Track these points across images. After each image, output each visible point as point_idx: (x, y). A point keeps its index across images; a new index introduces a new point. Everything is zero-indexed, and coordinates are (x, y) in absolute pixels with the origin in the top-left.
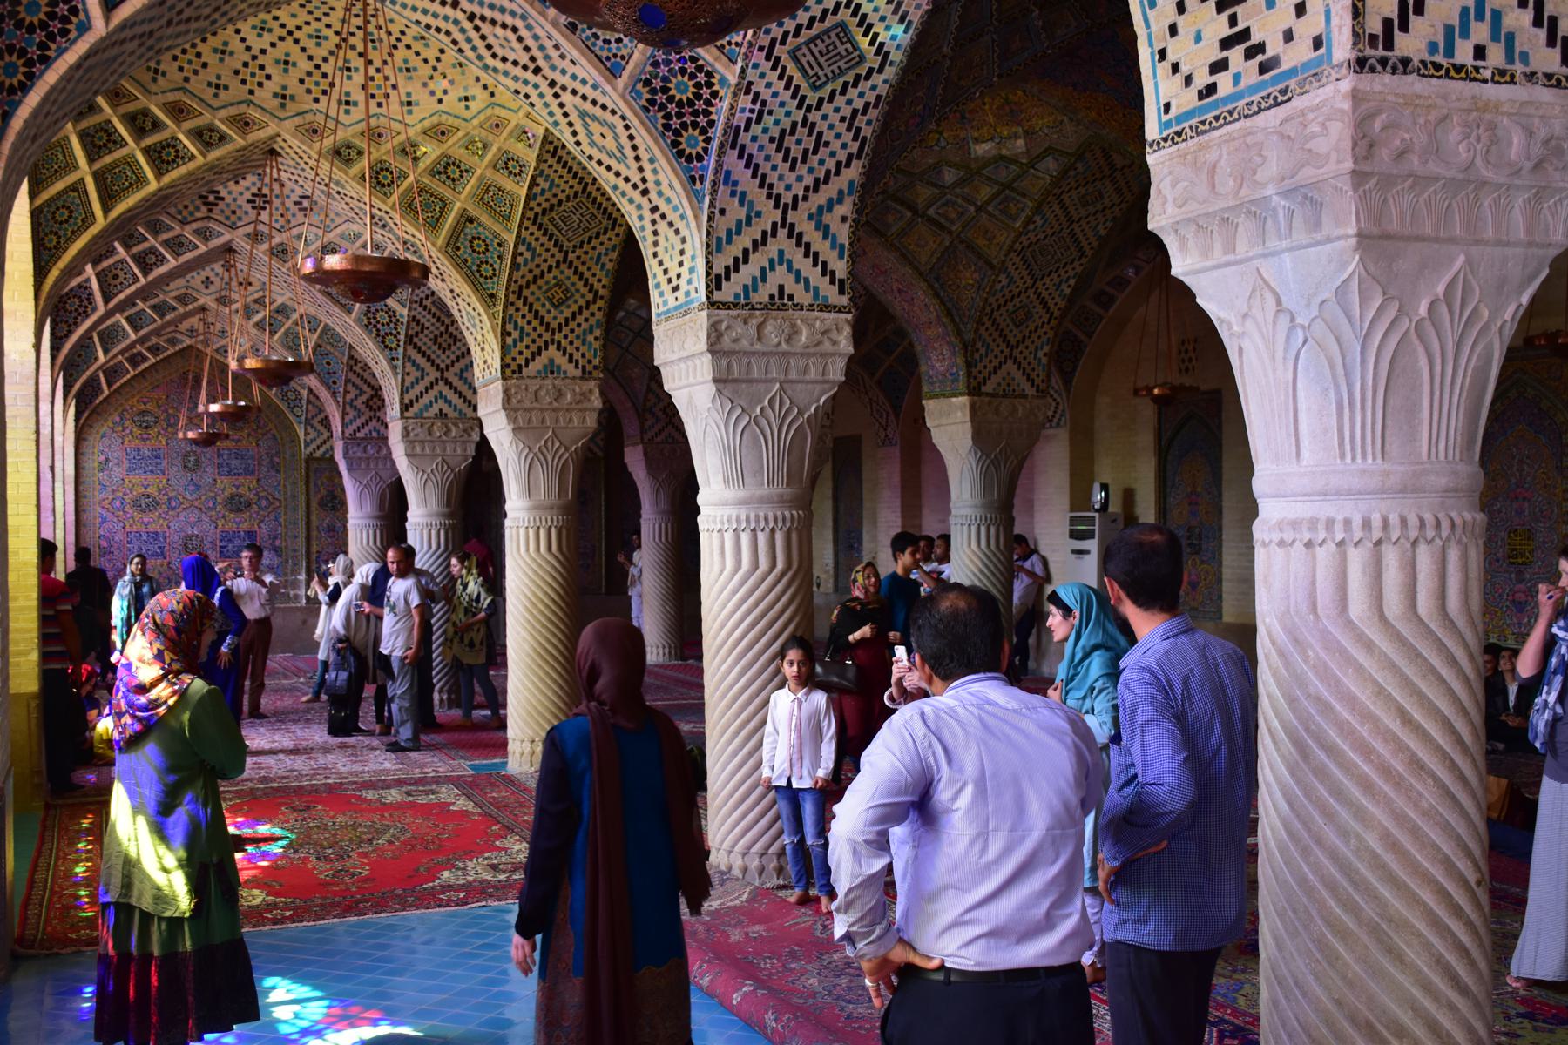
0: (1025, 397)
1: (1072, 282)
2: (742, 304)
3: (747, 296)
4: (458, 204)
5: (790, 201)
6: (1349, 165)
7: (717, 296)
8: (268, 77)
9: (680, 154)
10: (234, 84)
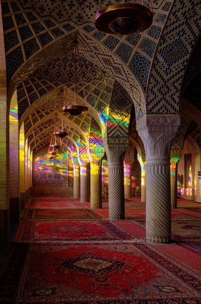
0: (178, 149)
1: (186, 129)
2: (112, 137)
3: (113, 136)
4: (82, 121)
5: (119, 122)
6: (146, 124)
7: (108, 136)
8: (55, 104)
9: (103, 116)
10: (50, 105)
